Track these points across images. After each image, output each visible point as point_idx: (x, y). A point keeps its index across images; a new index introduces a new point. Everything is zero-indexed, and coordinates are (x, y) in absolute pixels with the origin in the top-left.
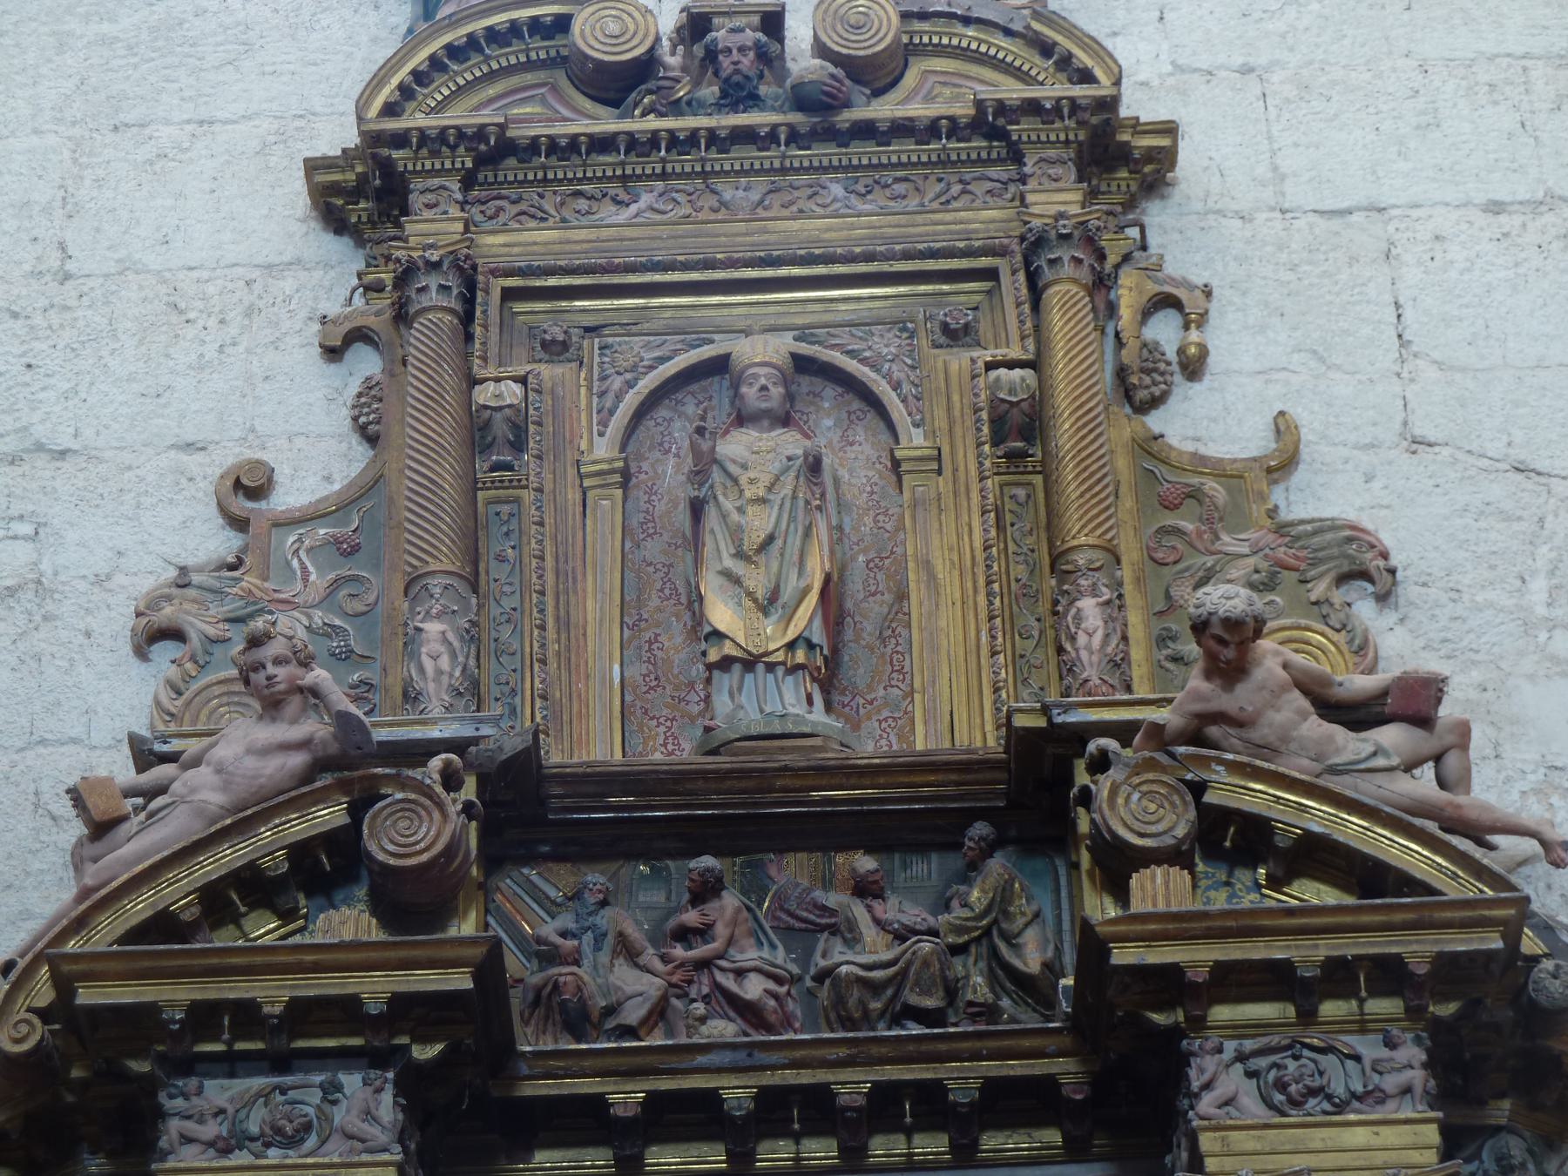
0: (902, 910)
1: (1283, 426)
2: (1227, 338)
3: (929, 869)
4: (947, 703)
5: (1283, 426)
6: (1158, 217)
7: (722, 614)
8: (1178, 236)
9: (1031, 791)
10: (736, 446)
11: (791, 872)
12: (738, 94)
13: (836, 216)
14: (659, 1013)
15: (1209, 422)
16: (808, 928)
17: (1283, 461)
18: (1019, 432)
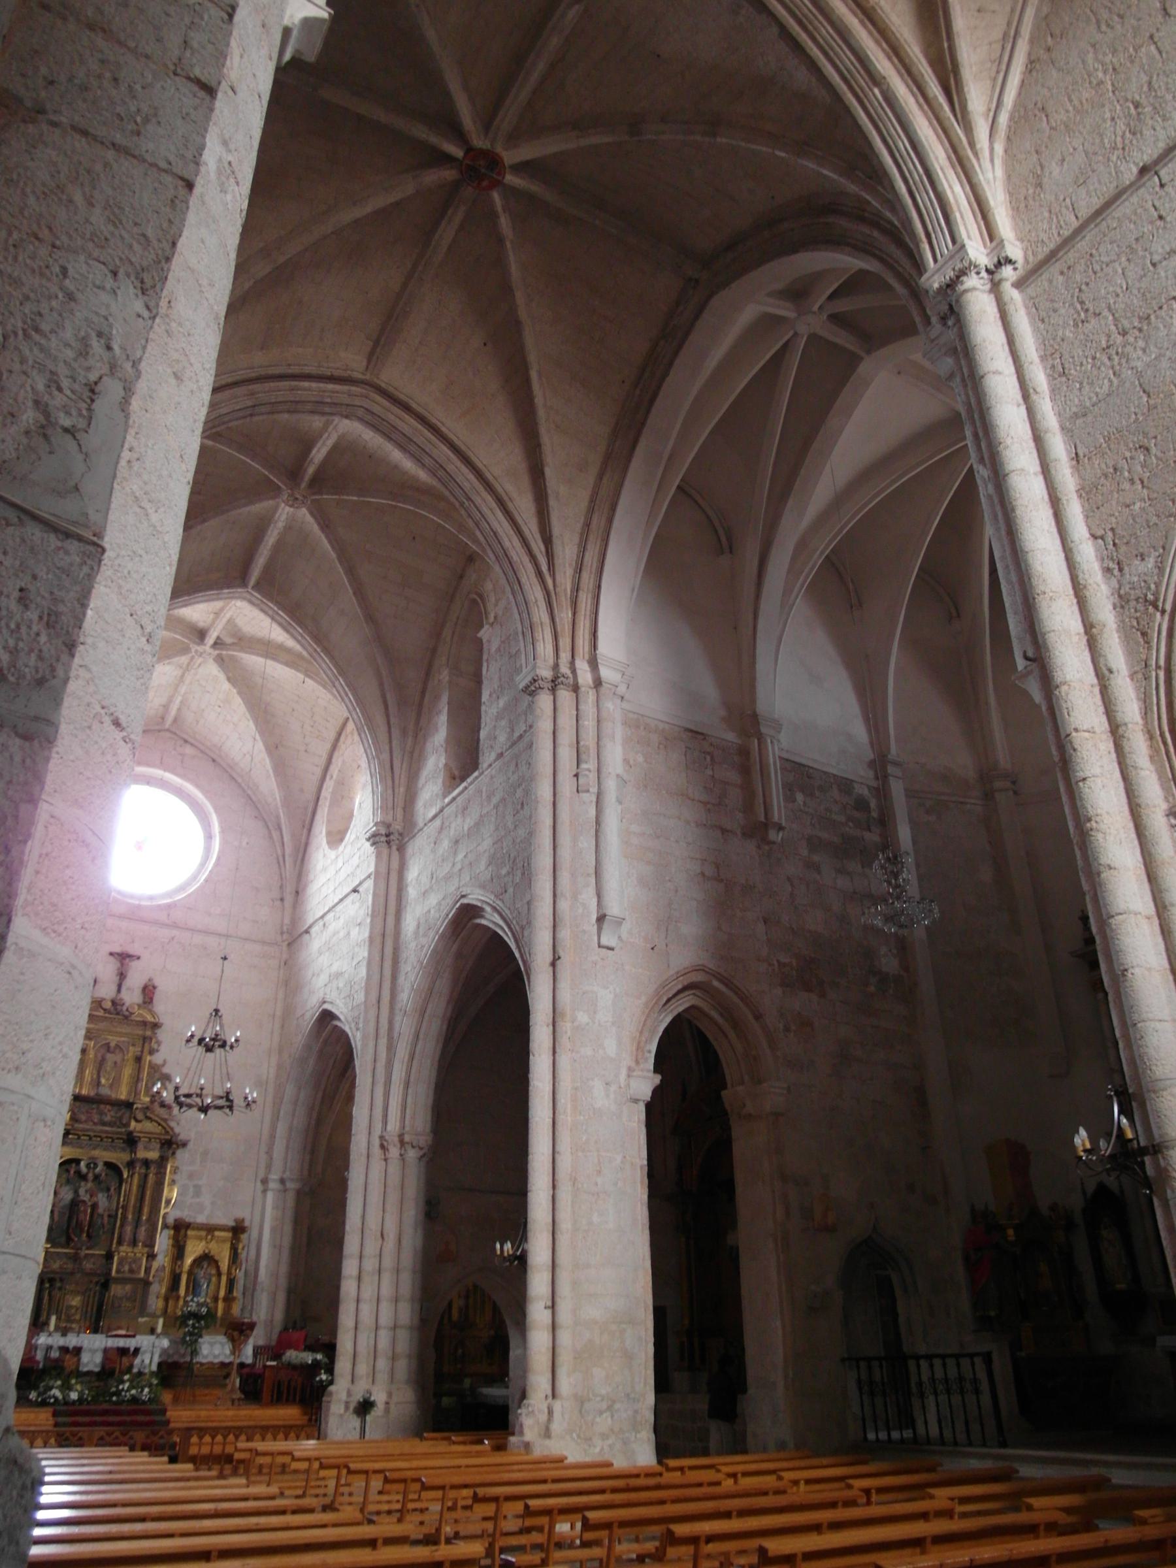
0: (112, 1113)
1: (165, 1061)
2: (163, 1048)
3: (116, 1108)
4: (123, 1095)
5: (165, 1061)
6: (158, 1031)
7: (103, 1081)
8: (161, 1034)
9: (129, 1105)
10: (109, 1056)
11: (102, 1106)
12: (118, 1014)
13: (125, 1029)
14: (86, 1121)
15: (157, 1059)
16: (101, 1113)
17: (163, 1065)
18: (138, 1059)
